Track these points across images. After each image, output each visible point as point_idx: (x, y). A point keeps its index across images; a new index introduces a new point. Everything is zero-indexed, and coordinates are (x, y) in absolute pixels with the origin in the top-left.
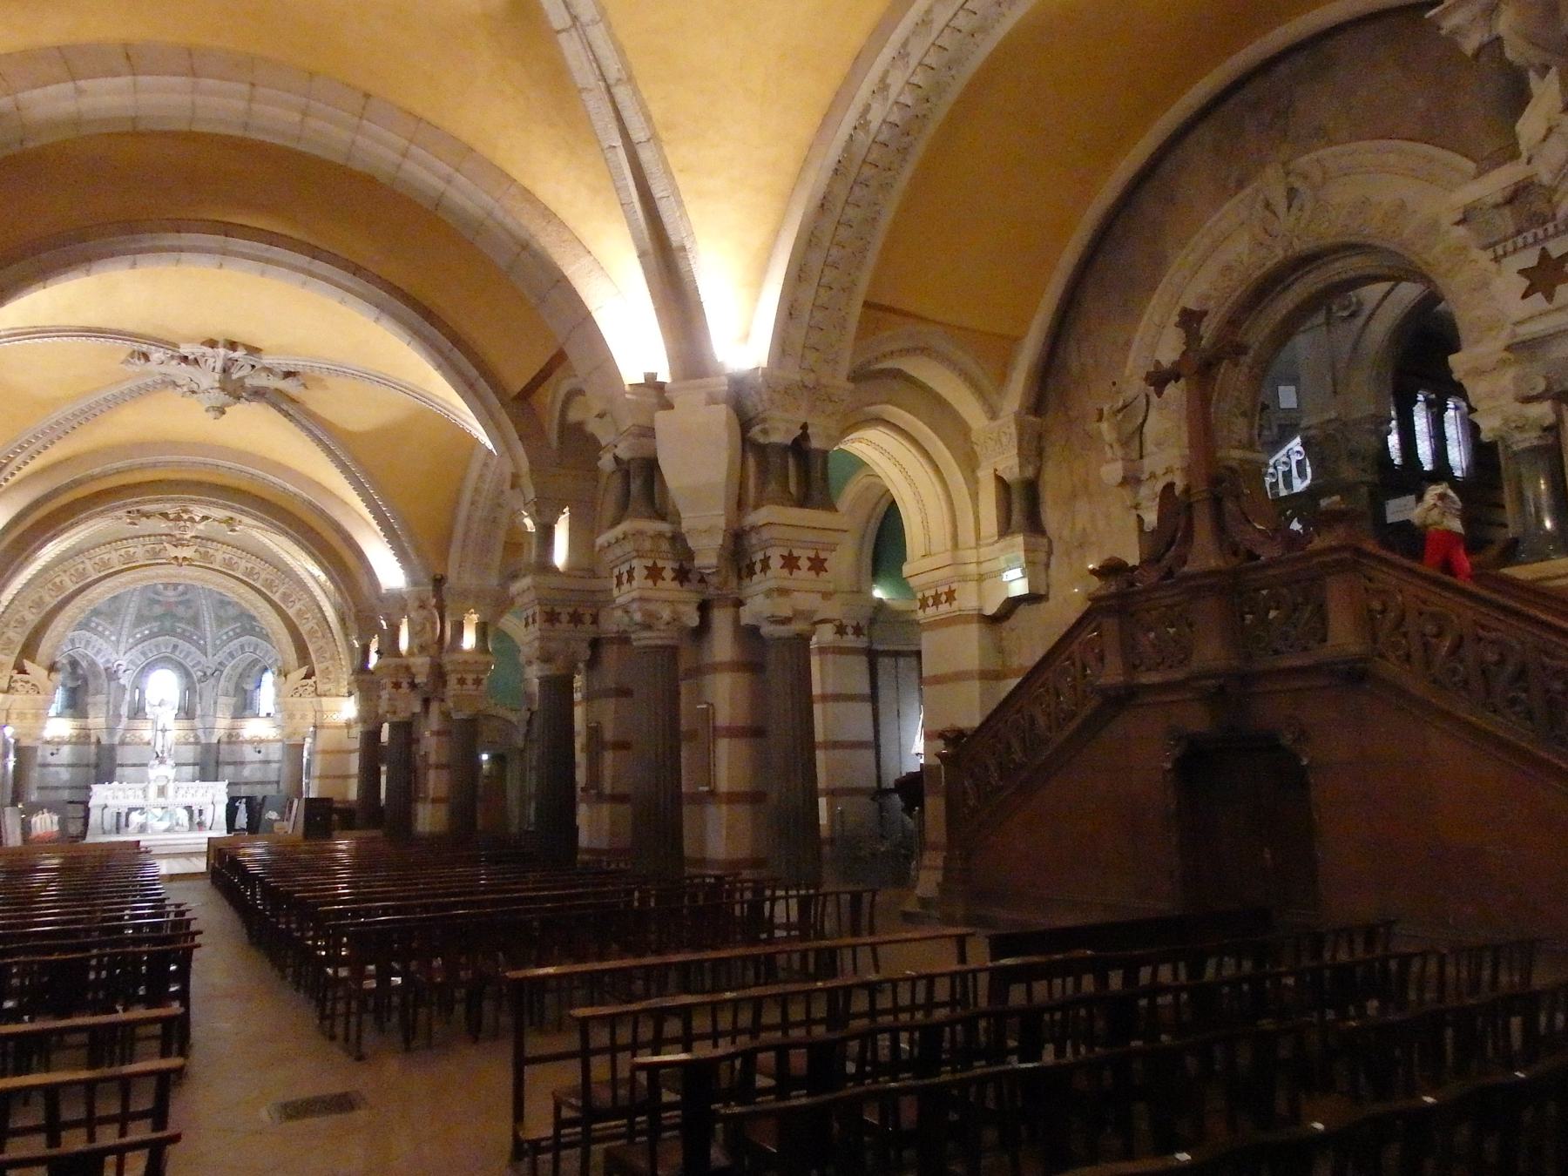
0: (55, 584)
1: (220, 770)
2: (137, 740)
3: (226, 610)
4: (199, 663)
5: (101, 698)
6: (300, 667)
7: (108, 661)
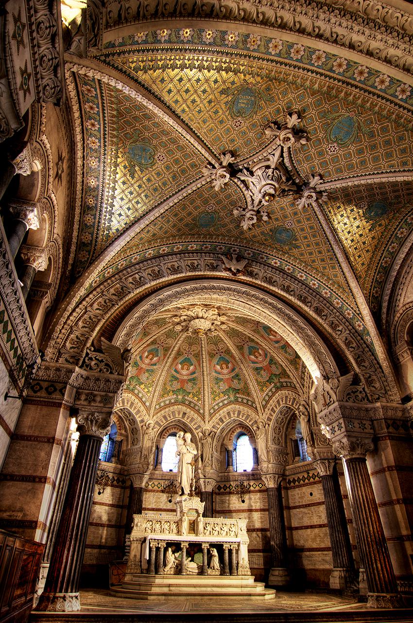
4: (199, 426)
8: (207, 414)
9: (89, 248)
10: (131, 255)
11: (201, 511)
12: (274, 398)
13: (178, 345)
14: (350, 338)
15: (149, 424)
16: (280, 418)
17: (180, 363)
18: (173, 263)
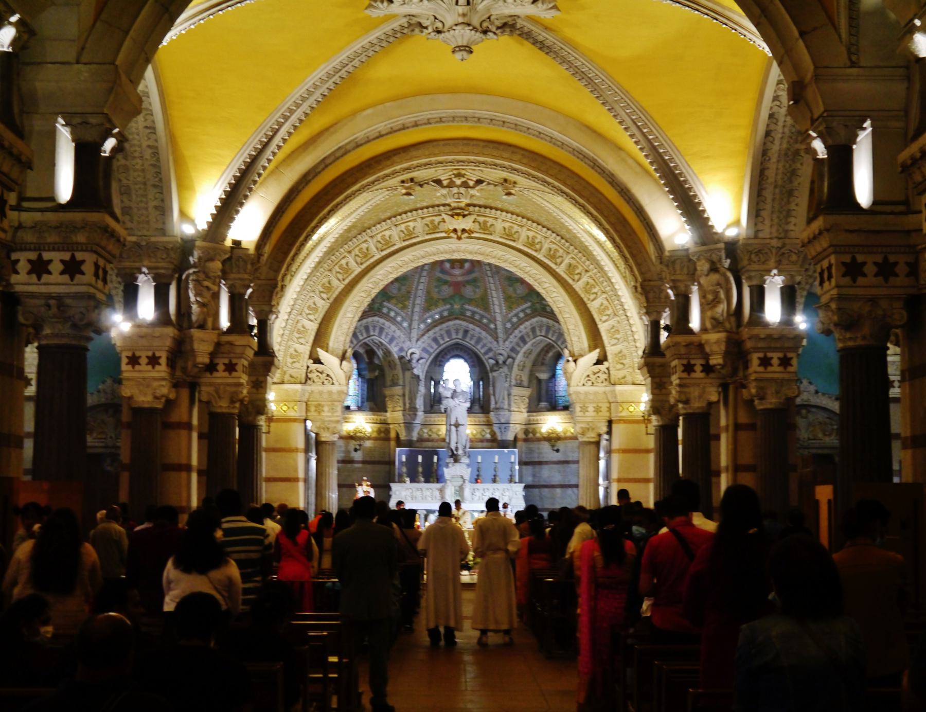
0: (341, 267)
2: (434, 436)
3: (515, 290)
4: (490, 350)
5: (398, 390)
6: (591, 350)
7: (401, 350)
11: (467, 477)
14: (605, 302)
15: (413, 353)
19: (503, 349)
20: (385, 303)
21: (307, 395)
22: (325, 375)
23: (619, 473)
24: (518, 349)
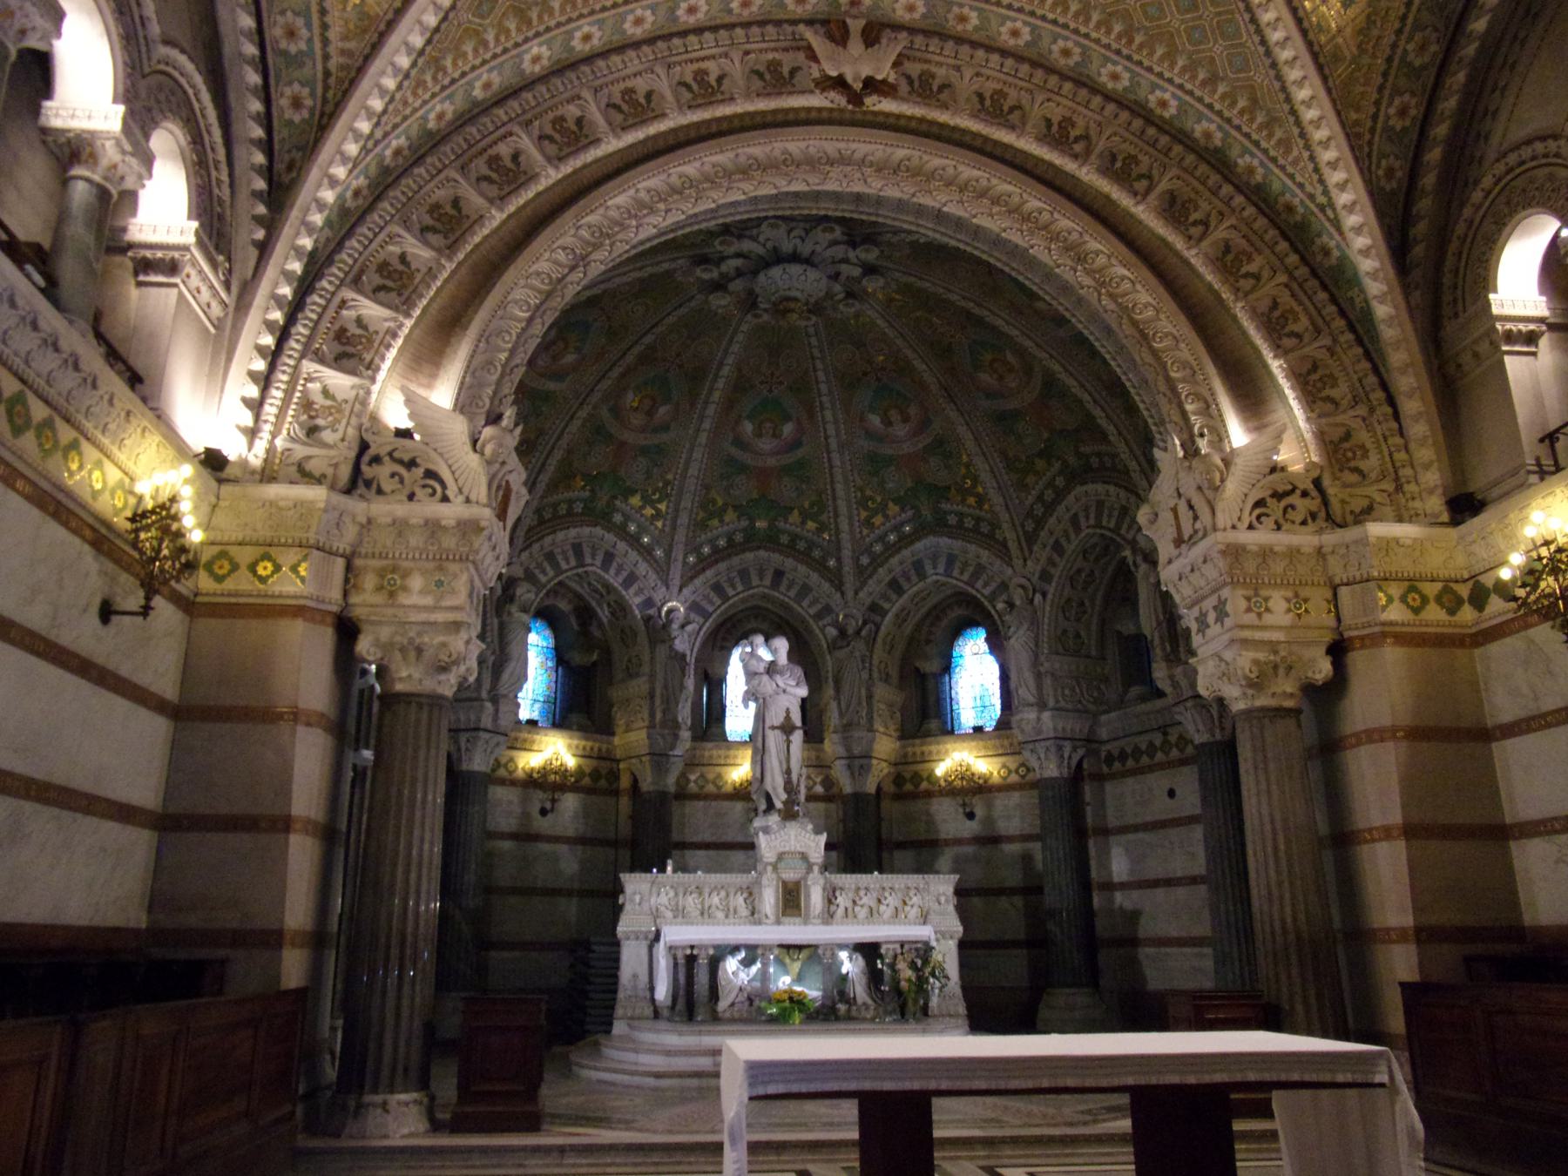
0: (494, 161)
1: (885, 855)
2: (711, 788)
4: (827, 610)
5: (639, 686)
7: (649, 603)
8: (848, 568)
9: (306, 71)
10: (464, 74)
12: (1061, 509)
13: (730, 360)
14: (1285, 299)
15: (670, 611)
16: (1079, 571)
17: (749, 417)
18: (629, 84)
19: (849, 611)
20: (618, 503)
21: (351, 532)
22: (420, 472)
23: (1404, 806)
24: (886, 606)
